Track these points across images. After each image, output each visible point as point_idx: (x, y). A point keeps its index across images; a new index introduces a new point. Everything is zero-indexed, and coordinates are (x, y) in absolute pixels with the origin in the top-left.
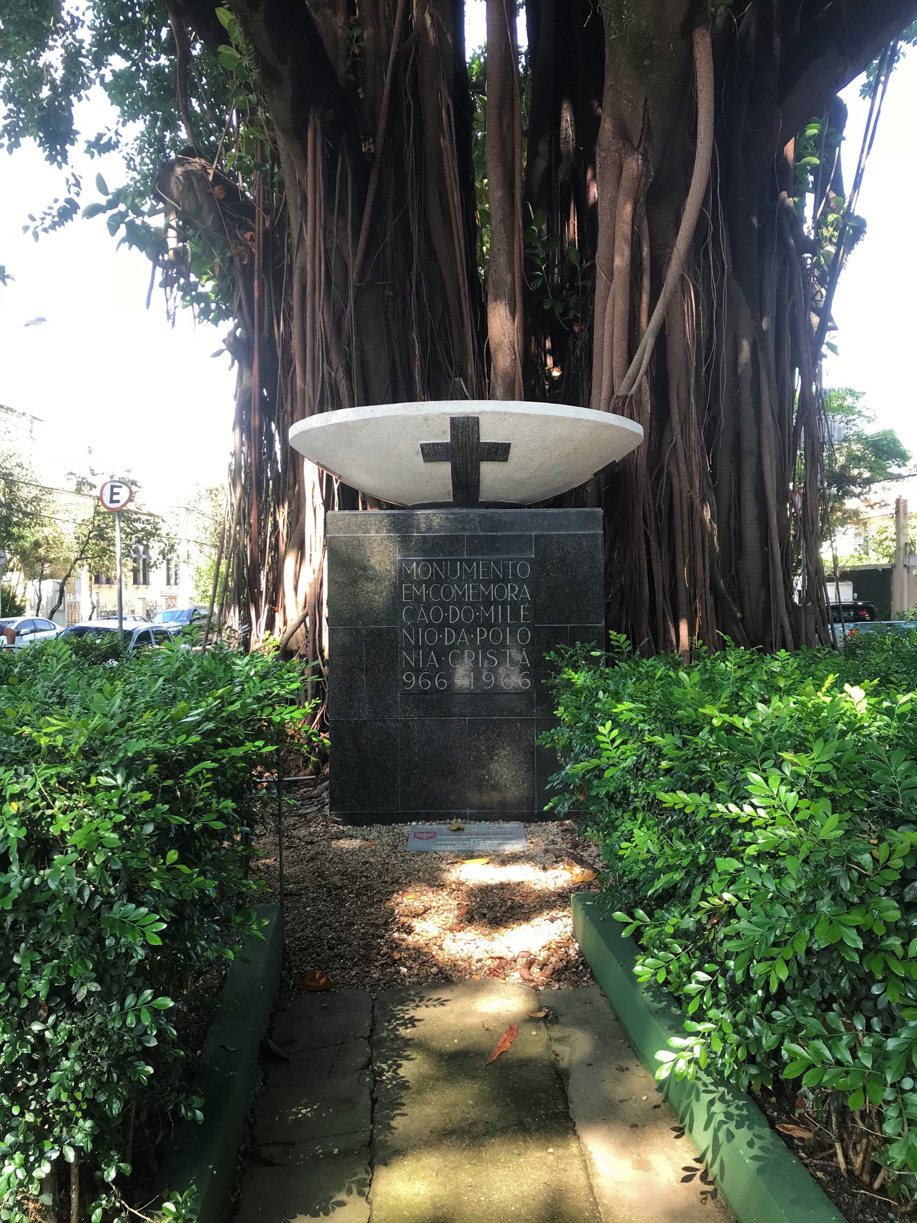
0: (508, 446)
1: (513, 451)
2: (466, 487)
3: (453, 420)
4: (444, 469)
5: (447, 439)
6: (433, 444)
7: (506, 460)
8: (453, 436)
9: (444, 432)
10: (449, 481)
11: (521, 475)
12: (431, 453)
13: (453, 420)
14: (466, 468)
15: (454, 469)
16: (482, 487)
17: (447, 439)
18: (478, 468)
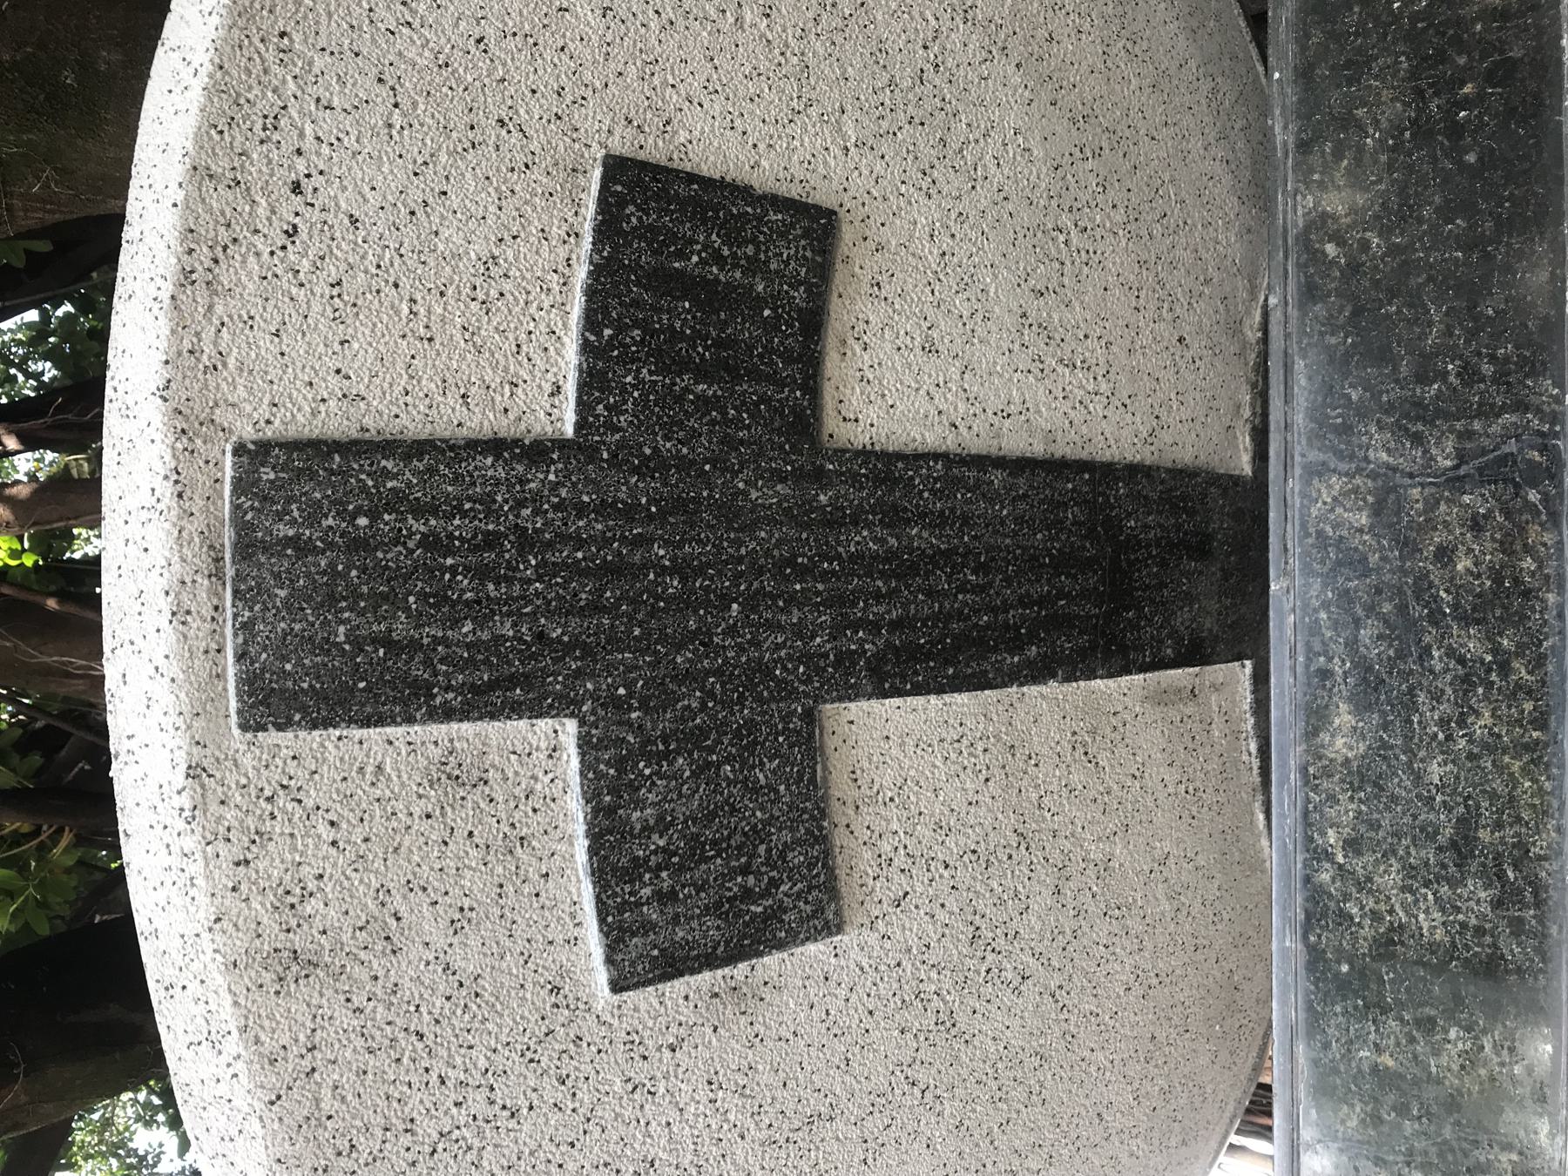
0: (616, 167)
1: (715, 140)
2: (1103, 570)
3: (271, 702)
4: (899, 755)
5: (543, 757)
6: (609, 871)
7: (816, 226)
8: (501, 687)
9: (452, 775)
10: (1046, 708)
11: (1006, 124)
12: (714, 877)
13: (271, 702)
14: (903, 567)
15: (897, 673)
16: (1115, 436)
17: (543, 757)
18: (887, 468)
